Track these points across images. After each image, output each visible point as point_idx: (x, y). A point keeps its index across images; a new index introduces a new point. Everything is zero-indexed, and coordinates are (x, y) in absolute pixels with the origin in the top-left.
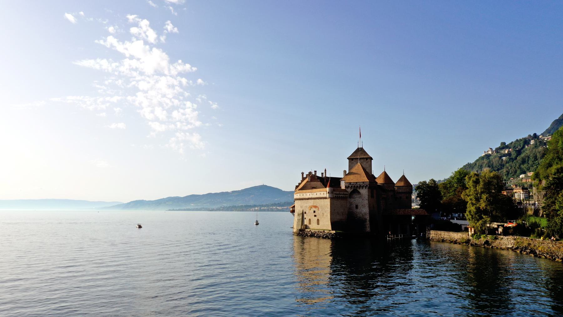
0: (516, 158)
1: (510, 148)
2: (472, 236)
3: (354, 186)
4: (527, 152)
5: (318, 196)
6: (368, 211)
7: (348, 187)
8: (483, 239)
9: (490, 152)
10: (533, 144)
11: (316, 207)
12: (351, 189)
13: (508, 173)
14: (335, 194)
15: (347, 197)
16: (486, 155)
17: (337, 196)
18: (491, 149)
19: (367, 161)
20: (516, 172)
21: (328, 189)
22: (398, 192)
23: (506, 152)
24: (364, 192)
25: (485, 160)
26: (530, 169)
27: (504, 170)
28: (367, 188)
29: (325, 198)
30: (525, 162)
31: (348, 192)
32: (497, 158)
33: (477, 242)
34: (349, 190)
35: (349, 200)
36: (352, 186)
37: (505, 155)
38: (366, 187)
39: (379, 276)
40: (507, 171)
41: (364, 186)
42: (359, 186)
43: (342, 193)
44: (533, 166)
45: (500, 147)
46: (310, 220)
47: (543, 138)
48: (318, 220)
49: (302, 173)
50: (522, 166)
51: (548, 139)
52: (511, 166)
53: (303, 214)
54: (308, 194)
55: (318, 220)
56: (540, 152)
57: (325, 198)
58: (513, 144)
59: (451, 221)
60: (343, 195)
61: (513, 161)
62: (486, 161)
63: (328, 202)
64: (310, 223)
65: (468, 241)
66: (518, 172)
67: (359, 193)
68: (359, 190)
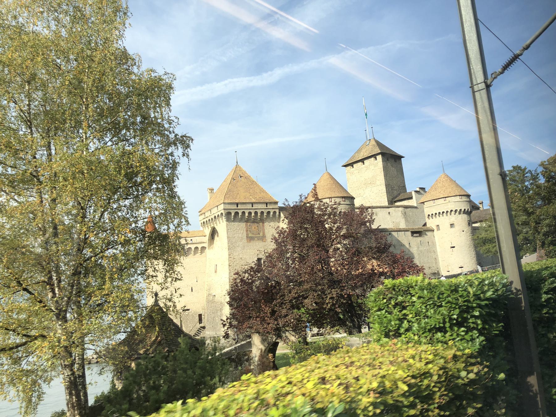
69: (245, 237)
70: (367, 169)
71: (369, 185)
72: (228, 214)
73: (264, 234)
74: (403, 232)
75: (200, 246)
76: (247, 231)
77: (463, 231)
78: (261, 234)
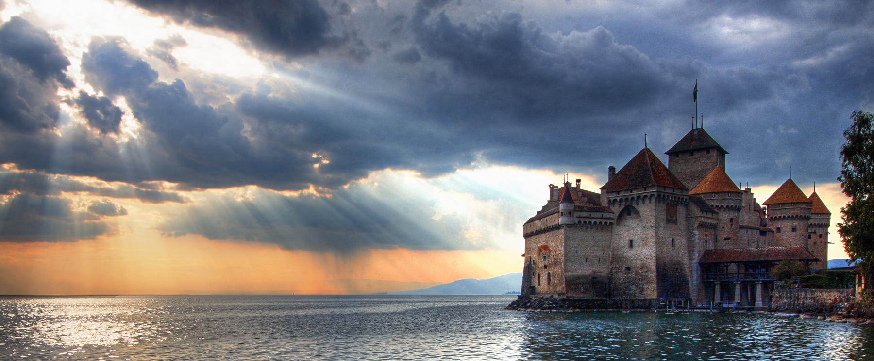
3: (627, 199)
6: (655, 252)
7: (615, 200)
12: (620, 205)
14: (577, 217)
15: (611, 224)
17: (582, 220)
19: (709, 155)
22: (772, 217)
28: (653, 200)
29: (558, 227)
31: (613, 213)
34: (617, 209)
35: (616, 229)
36: (621, 200)
38: (650, 199)
39: (18, 331)
41: (646, 196)
42: (635, 196)
43: (599, 215)
49: (550, 185)
57: (558, 227)
60: (601, 220)
64: (539, 284)
67: (637, 213)
68: (636, 207)
69: (665, 219)
70: (695, 161)
71: (696, 179)
72: (659, 196)
73: (676, 218)
74: (755, 230)
75: (609, 222)
76: (667, 213)
77: (803, 236)
78: (674, 218)
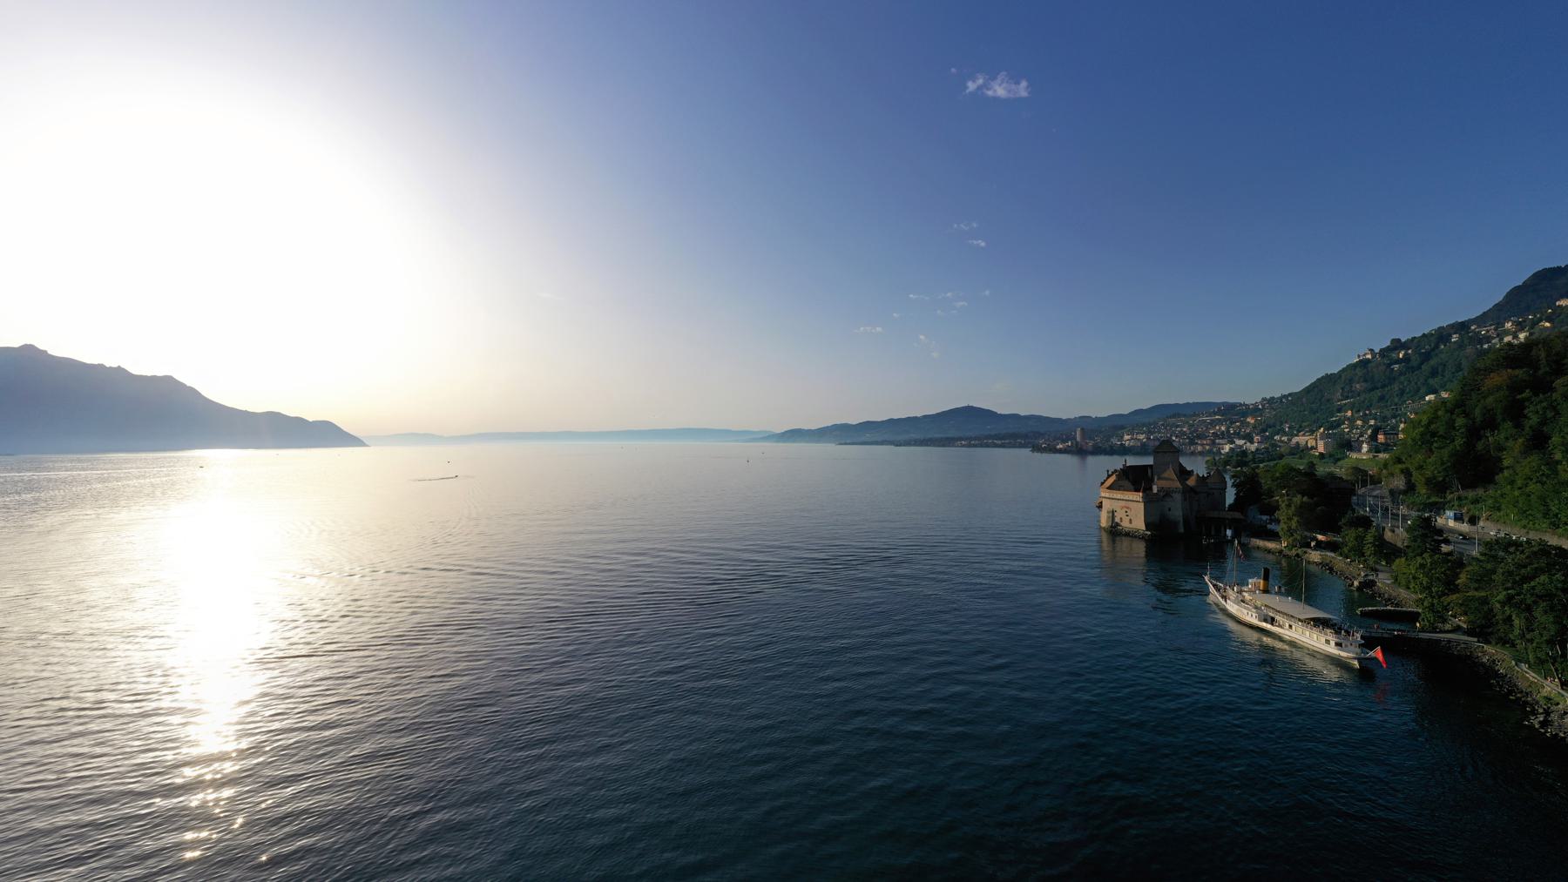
0: (1419, 367)
1: (1409, 349)
2: (1285, 547)
4: (1443, 356)
5: (1131, 498)
8: (1294, 552)
9: (1369, 356)
10: (1455, 342)
11: (1128, 508)
13: (1402, 392)
16: (1360, 361)
18: (1372, 350)
20: (1418, 390)
21: (1141, 494)
23: (1401, 356)
24: (1178, 497)
25: (1358, 369)
26: (1445, 385)
27: (1396, 387)
30: (1437, 373)
32: (1383, 368)
33: (1290, 553)
34: (1162, 494)
37: (1398, 361)
40: (1400, 389)
44: (1452, 381)
45: (1388, 346)
46: (1121, 519)
47: (1477, 330)
48: (1131, 520)
50: (1431, 381)
51: (1488, 331)
52: (1409, 381)
53: (1113, 512)
54: (1118, 495)
55: (1131, 520)
56: (1467, 358)
58: (1416, 341)
59: (1269, 526)
61: (1413, 372)
62: (1359, 372)
63: (1141, 506)
65: (1281, 552)
66: (1423, 390)
